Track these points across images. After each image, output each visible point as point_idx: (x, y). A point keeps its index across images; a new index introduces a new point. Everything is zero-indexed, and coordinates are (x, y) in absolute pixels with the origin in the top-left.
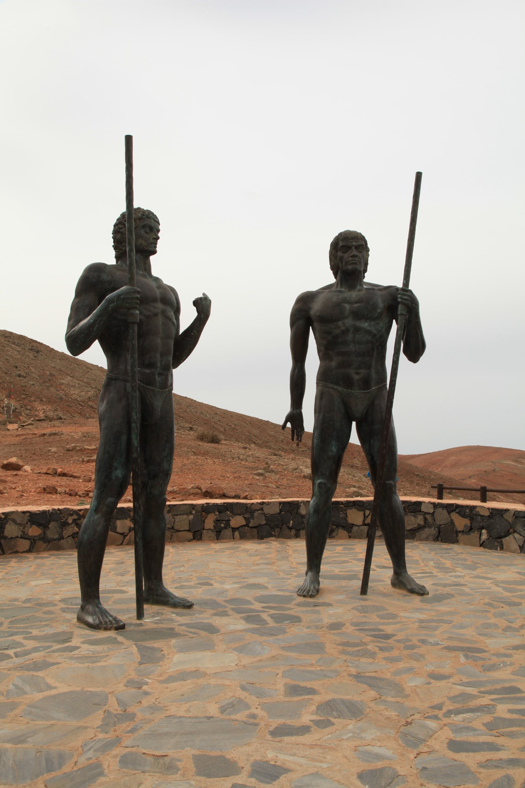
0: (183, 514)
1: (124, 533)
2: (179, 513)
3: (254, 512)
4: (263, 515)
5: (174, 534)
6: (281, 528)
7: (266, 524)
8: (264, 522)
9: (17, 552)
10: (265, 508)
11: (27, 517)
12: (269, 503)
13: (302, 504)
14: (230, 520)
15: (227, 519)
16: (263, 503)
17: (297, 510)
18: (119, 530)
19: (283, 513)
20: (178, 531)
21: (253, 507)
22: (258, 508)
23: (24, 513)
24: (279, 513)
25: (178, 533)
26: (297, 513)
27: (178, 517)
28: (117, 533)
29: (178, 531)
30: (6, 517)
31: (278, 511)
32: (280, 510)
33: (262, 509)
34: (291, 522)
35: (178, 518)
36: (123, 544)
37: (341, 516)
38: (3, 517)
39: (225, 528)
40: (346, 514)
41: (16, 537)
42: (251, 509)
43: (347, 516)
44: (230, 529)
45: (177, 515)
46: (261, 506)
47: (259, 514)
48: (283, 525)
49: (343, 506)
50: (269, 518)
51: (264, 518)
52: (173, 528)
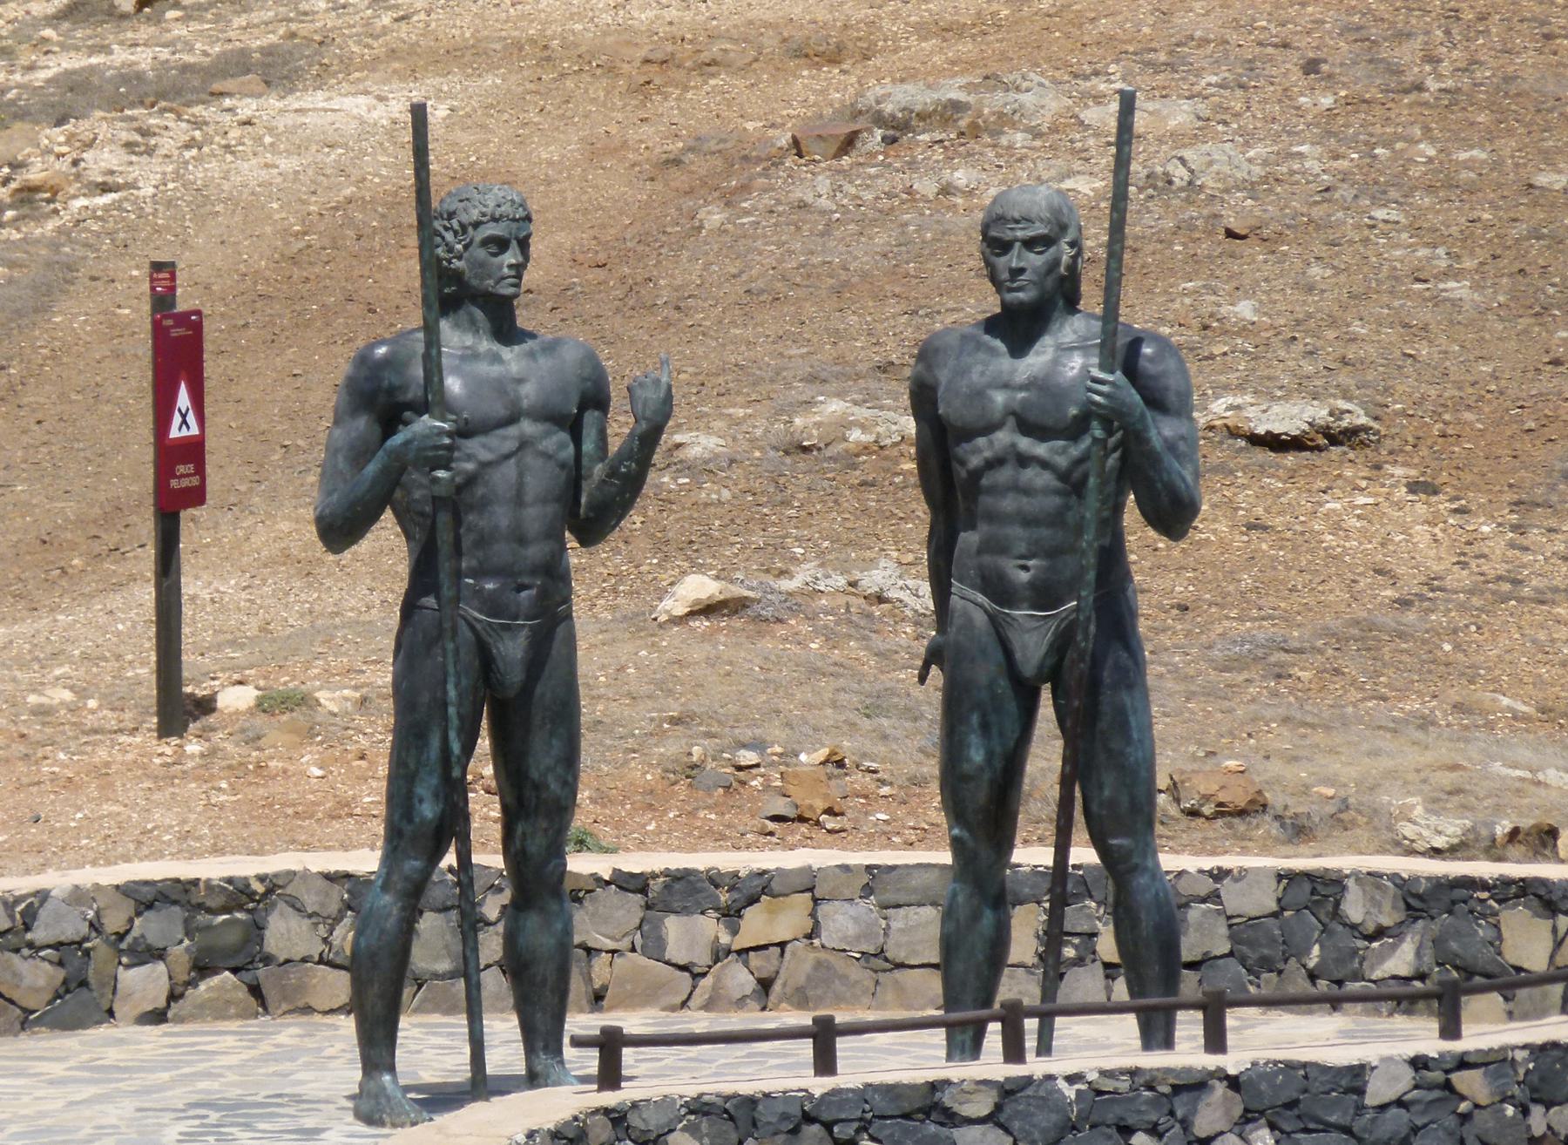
0: (920, 905)
1: (694, 964)
2: (902, 898)
3: (1186, 905)
4: (1222, 921)
5: (882, 977)
6: (1280, 972)
7: (1231, 954)
8: (1225, 948)
9: (308, 1010)
10: (1227, 888)
11: (340, 893)
12: (1243, 873)
13: (1350, 883)
14: (1095, 935)
15: (1085, 928)
16: (1219, 875)
17: (1337, 904)
18: (676, 952)
19: (1287, 914)
20: (901, 966)
21: (1184, 887)
22: (1203, 893)
23: (330, 878)
24: (1275, 915)
25: (898, 974)
26: (1336, 913)
27: (902, 911)
28: (667, 963)
29: (901, 966)
30: (269, 891)
31: (1274, 906)
32: (1279, 900)
33: (1214, 897)
34: (1316, 950)
35: (899, 919)
36: (691, 1003)
37: (1481, 932)
38: (259, 888)
39: (1079, 962)
40: (1497, 926)
41: (304, 960)
42: (1178, 894)
43: (1500, 937)
44: (1098, 963)
45: (898, 906)
46: (1208, 885)
47: (1205, 913)
48: (1286, 961)
49: (1485, 895)
50: (1242, 930)
51: (1224, 931)
52: (880, 953)
